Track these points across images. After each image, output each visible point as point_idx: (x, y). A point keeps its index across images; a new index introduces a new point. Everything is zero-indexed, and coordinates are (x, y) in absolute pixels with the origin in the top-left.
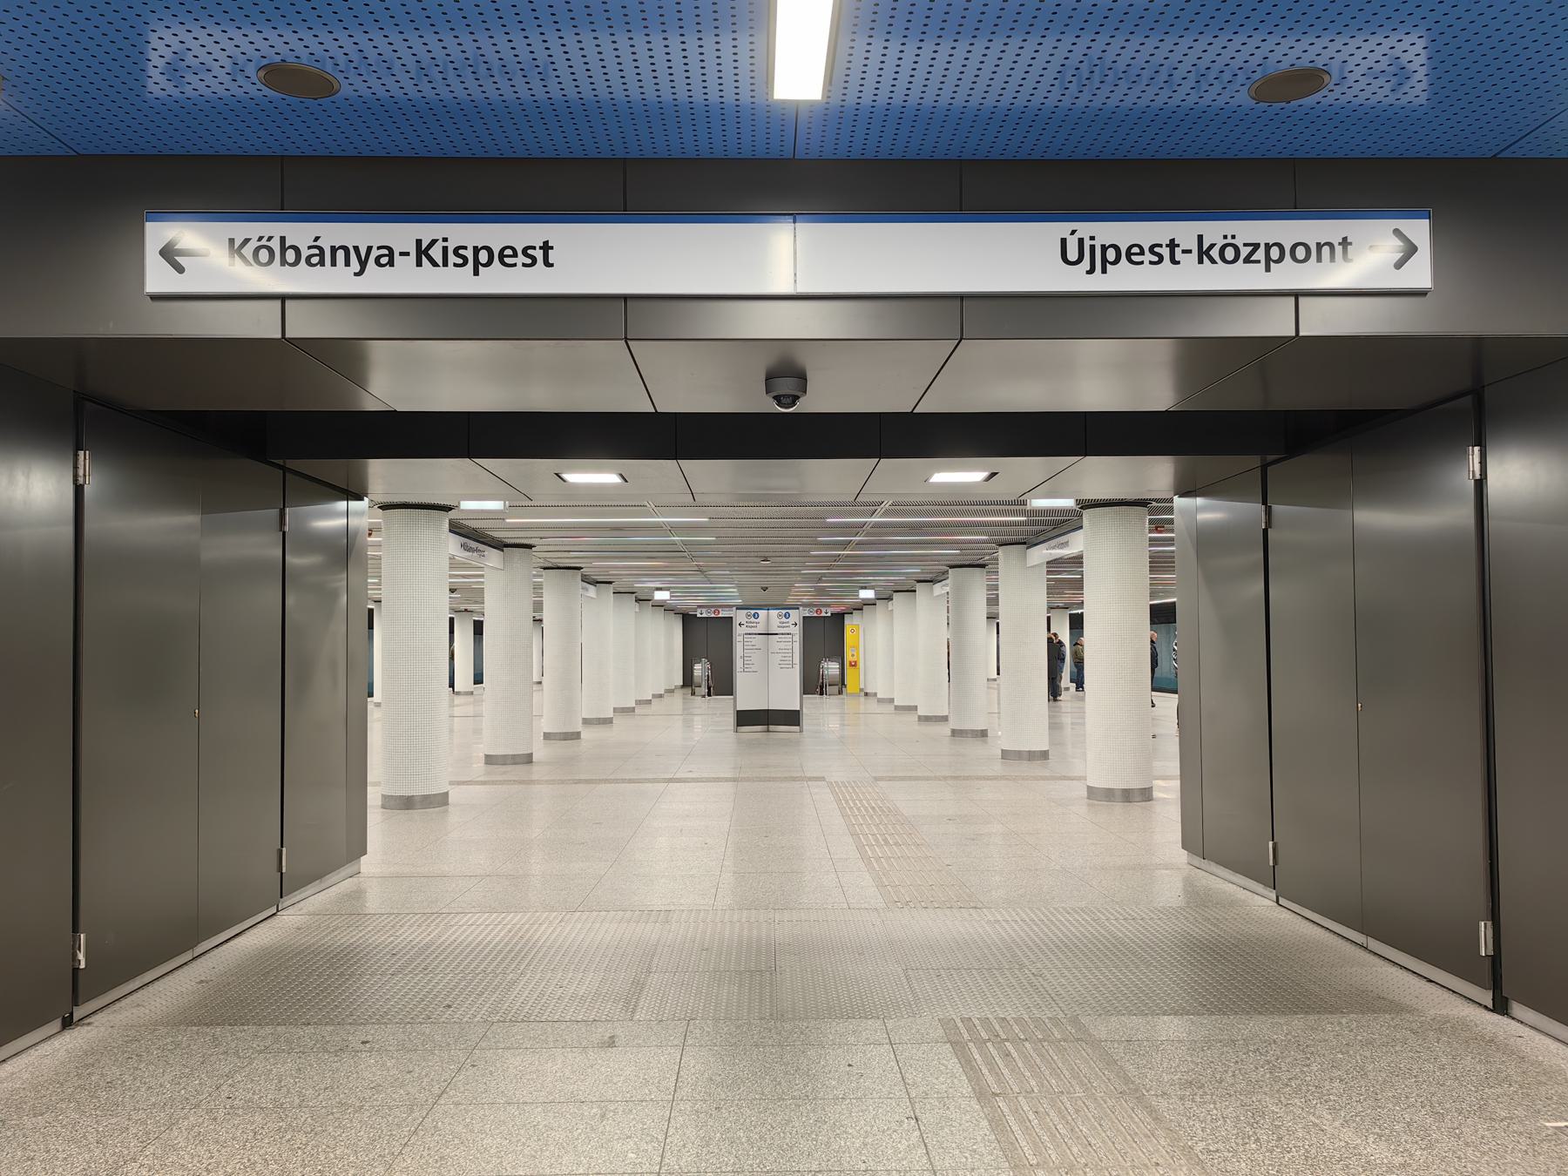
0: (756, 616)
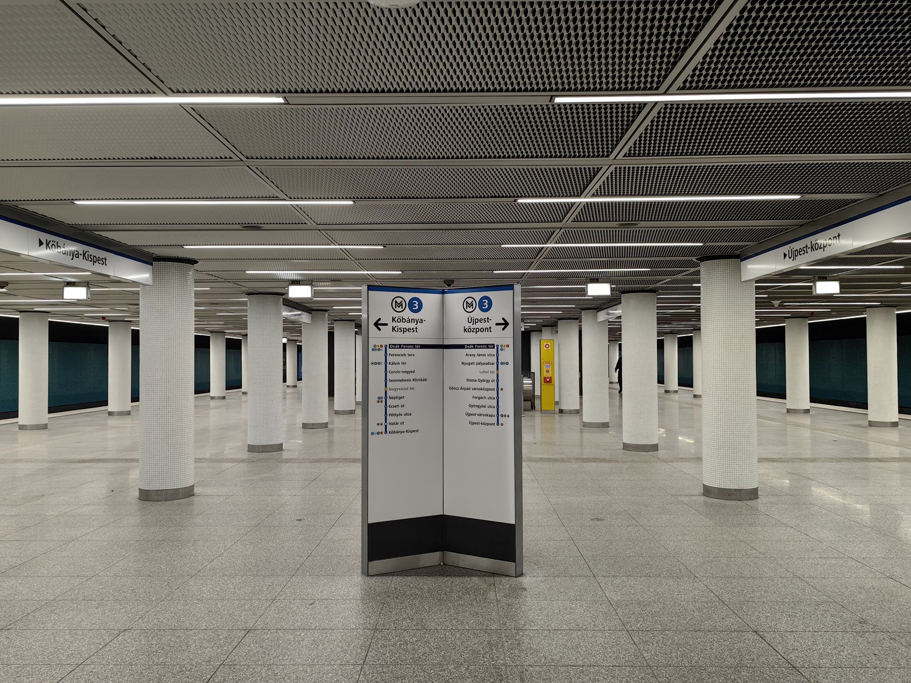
0: (415, 306)
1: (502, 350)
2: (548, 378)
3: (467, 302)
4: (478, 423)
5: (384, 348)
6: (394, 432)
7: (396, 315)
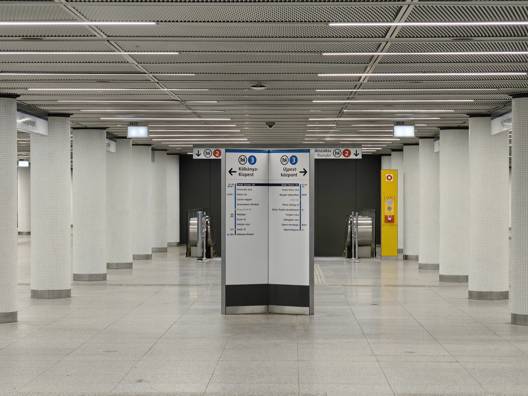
0: (252, 161)
1: (303, 187)
2: (390, 216)
3: (283, 159)
4: (289, 230)
5: (234, 185)
6: (240, 234)
7: (242, 166)
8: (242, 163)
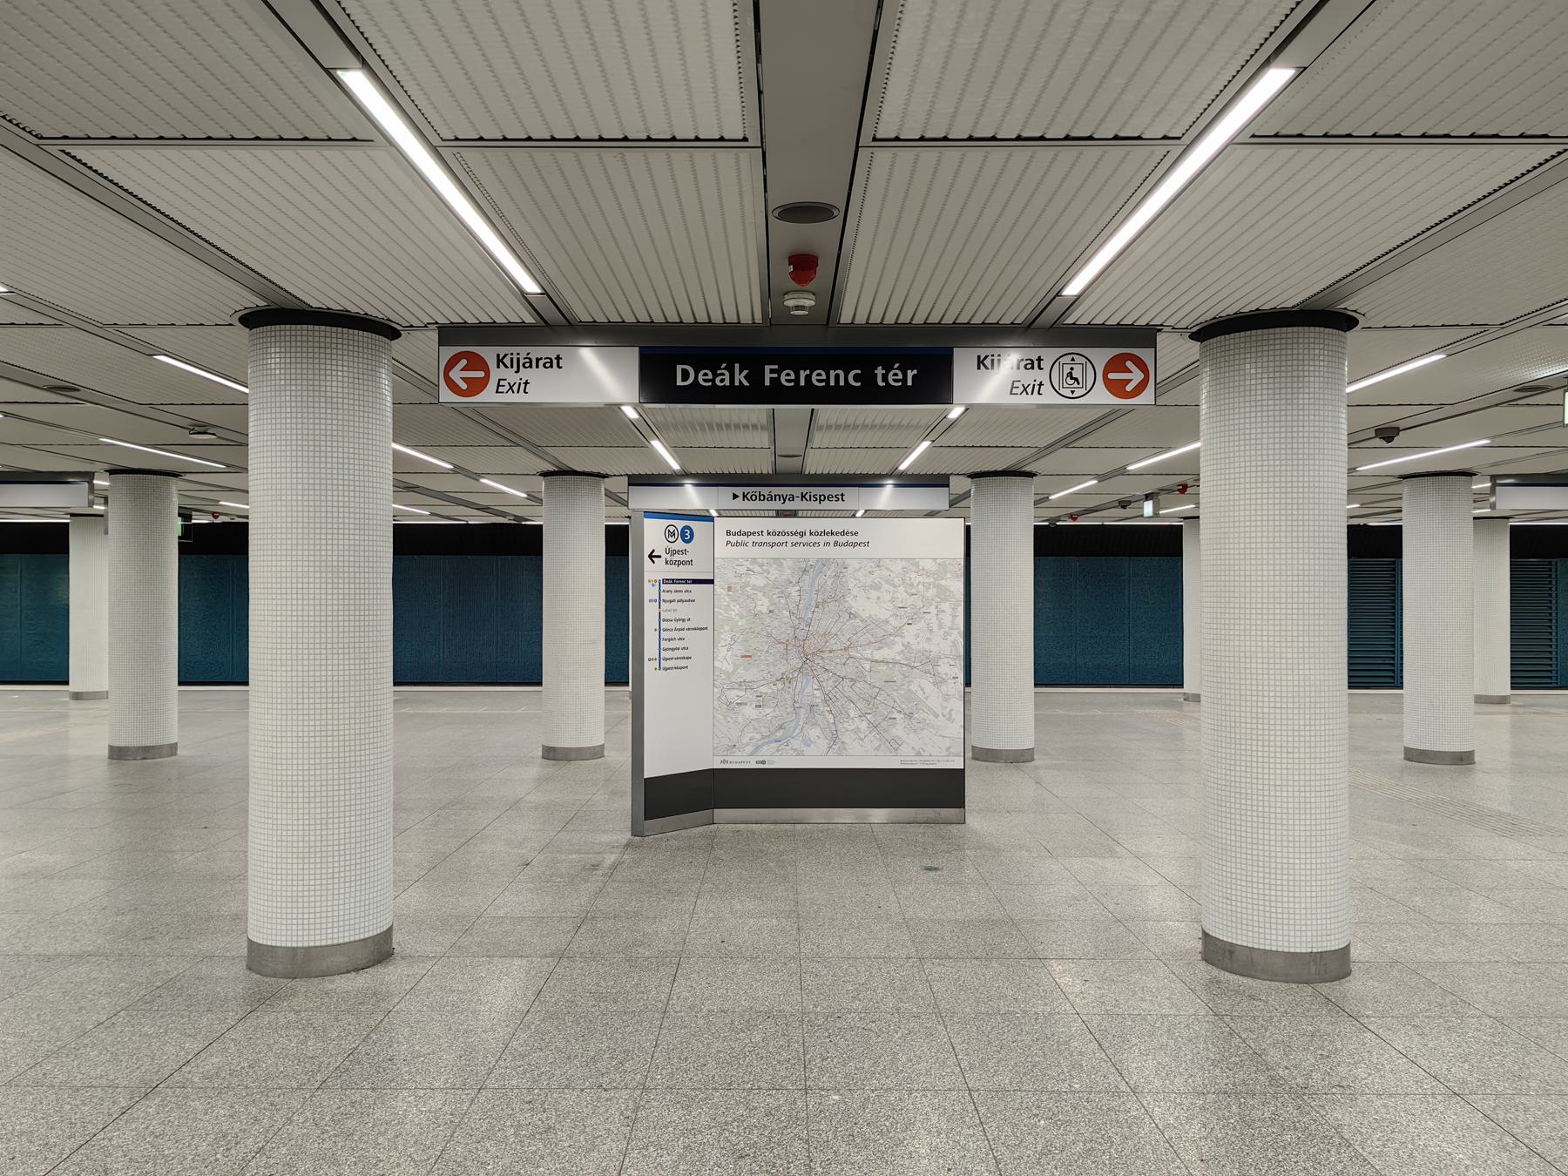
8: (672, 539)
